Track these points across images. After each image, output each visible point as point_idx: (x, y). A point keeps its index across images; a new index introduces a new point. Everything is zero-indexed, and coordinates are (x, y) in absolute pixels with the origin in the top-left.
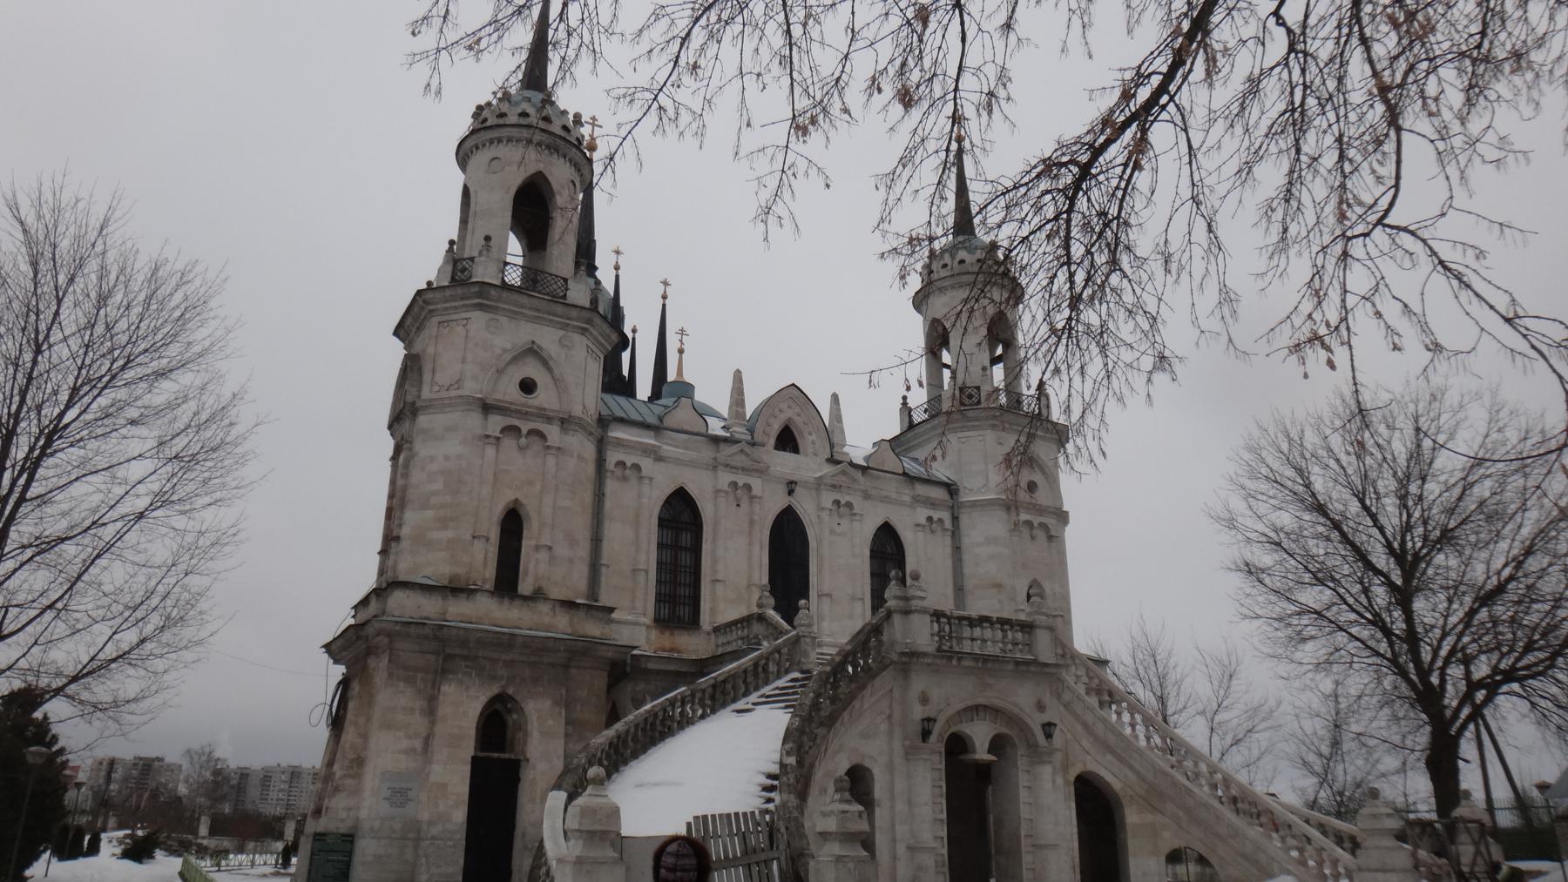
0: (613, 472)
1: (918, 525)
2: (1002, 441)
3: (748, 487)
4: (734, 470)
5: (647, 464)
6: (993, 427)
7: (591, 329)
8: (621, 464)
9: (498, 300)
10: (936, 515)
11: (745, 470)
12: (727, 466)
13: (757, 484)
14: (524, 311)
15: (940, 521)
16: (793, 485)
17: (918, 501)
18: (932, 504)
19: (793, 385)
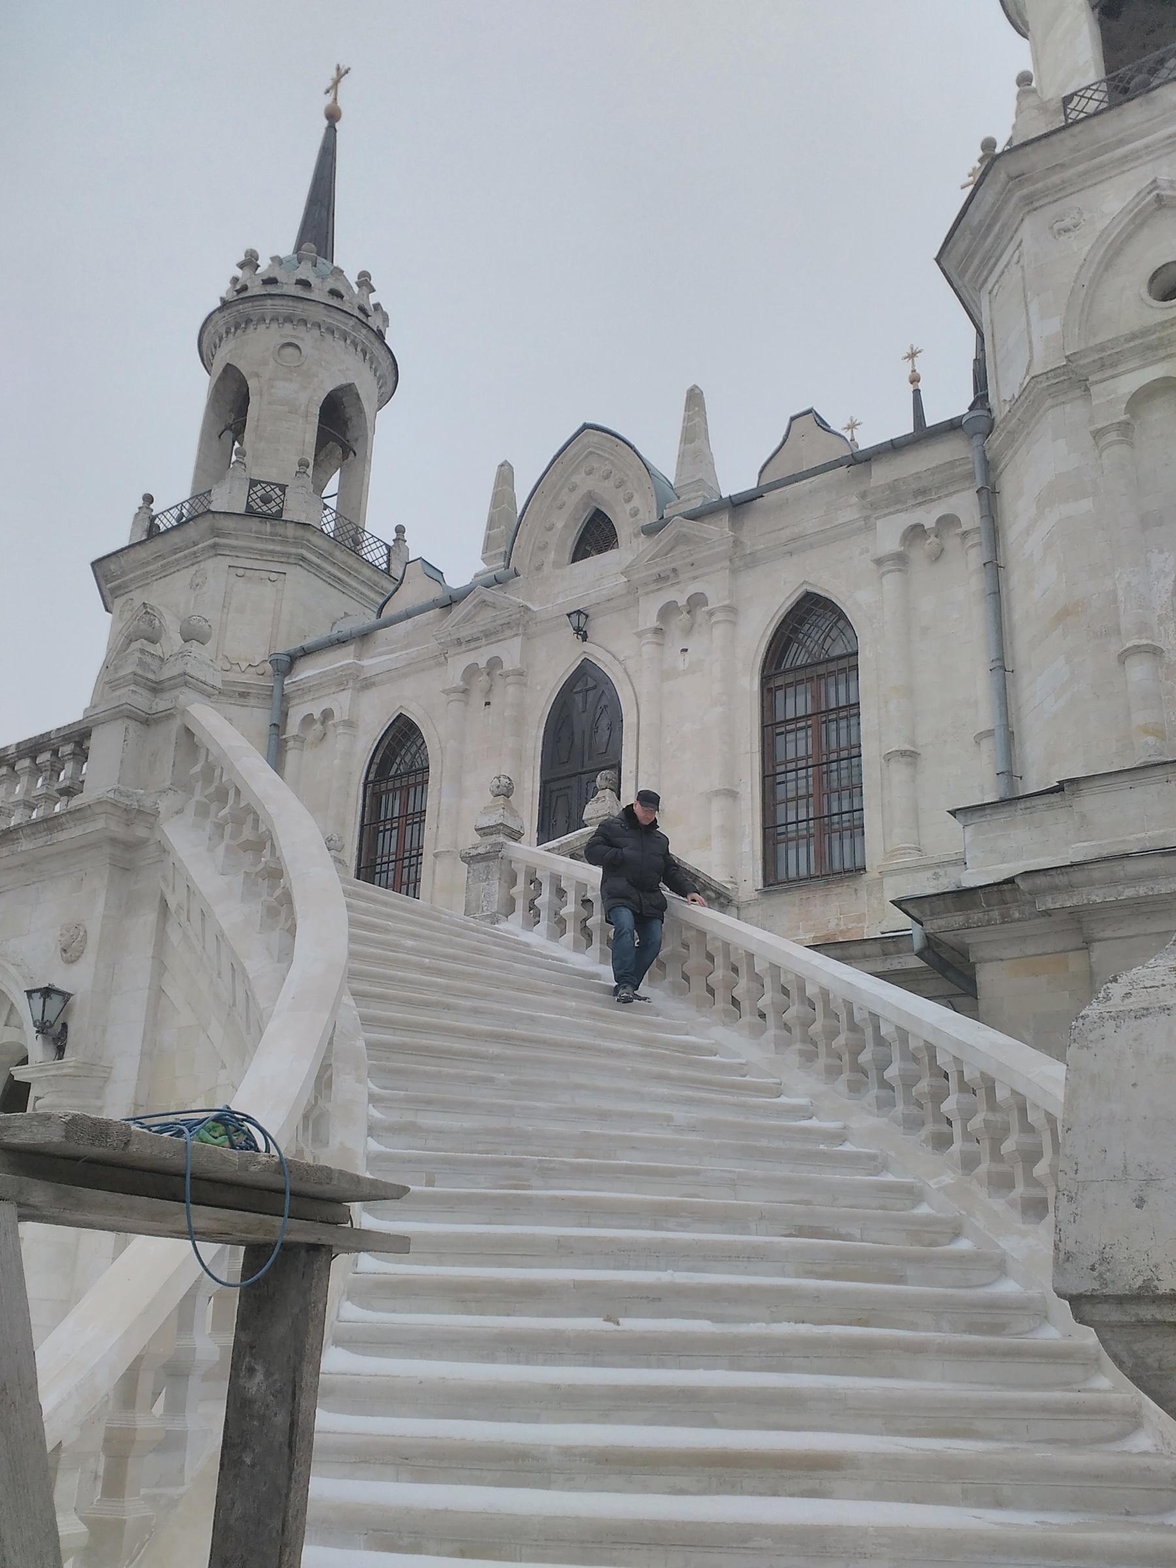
0: (295, 737)
1: (879, 562)
2: (1068, 222)
3: (495, 663)
4: (473, 645)
5: (340, 703)
6: (1031, 203)
7: (217, 540)
8: (308, 720)
9: (124, 574)
10: (928, 517)
11: (489, 635)
12: (459, 642)
13: (510, 652)
14: (149, 569)
15: (949, 521)
16: (583, 617)
17: (874, 506)
18: (923, 494)
19: (586, 427)
